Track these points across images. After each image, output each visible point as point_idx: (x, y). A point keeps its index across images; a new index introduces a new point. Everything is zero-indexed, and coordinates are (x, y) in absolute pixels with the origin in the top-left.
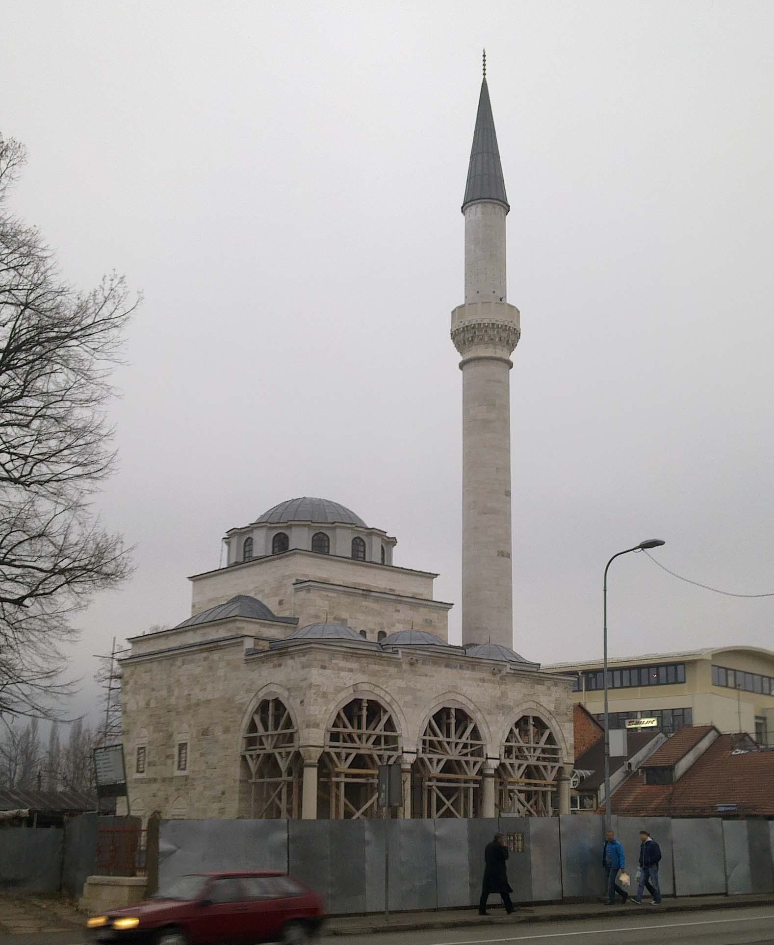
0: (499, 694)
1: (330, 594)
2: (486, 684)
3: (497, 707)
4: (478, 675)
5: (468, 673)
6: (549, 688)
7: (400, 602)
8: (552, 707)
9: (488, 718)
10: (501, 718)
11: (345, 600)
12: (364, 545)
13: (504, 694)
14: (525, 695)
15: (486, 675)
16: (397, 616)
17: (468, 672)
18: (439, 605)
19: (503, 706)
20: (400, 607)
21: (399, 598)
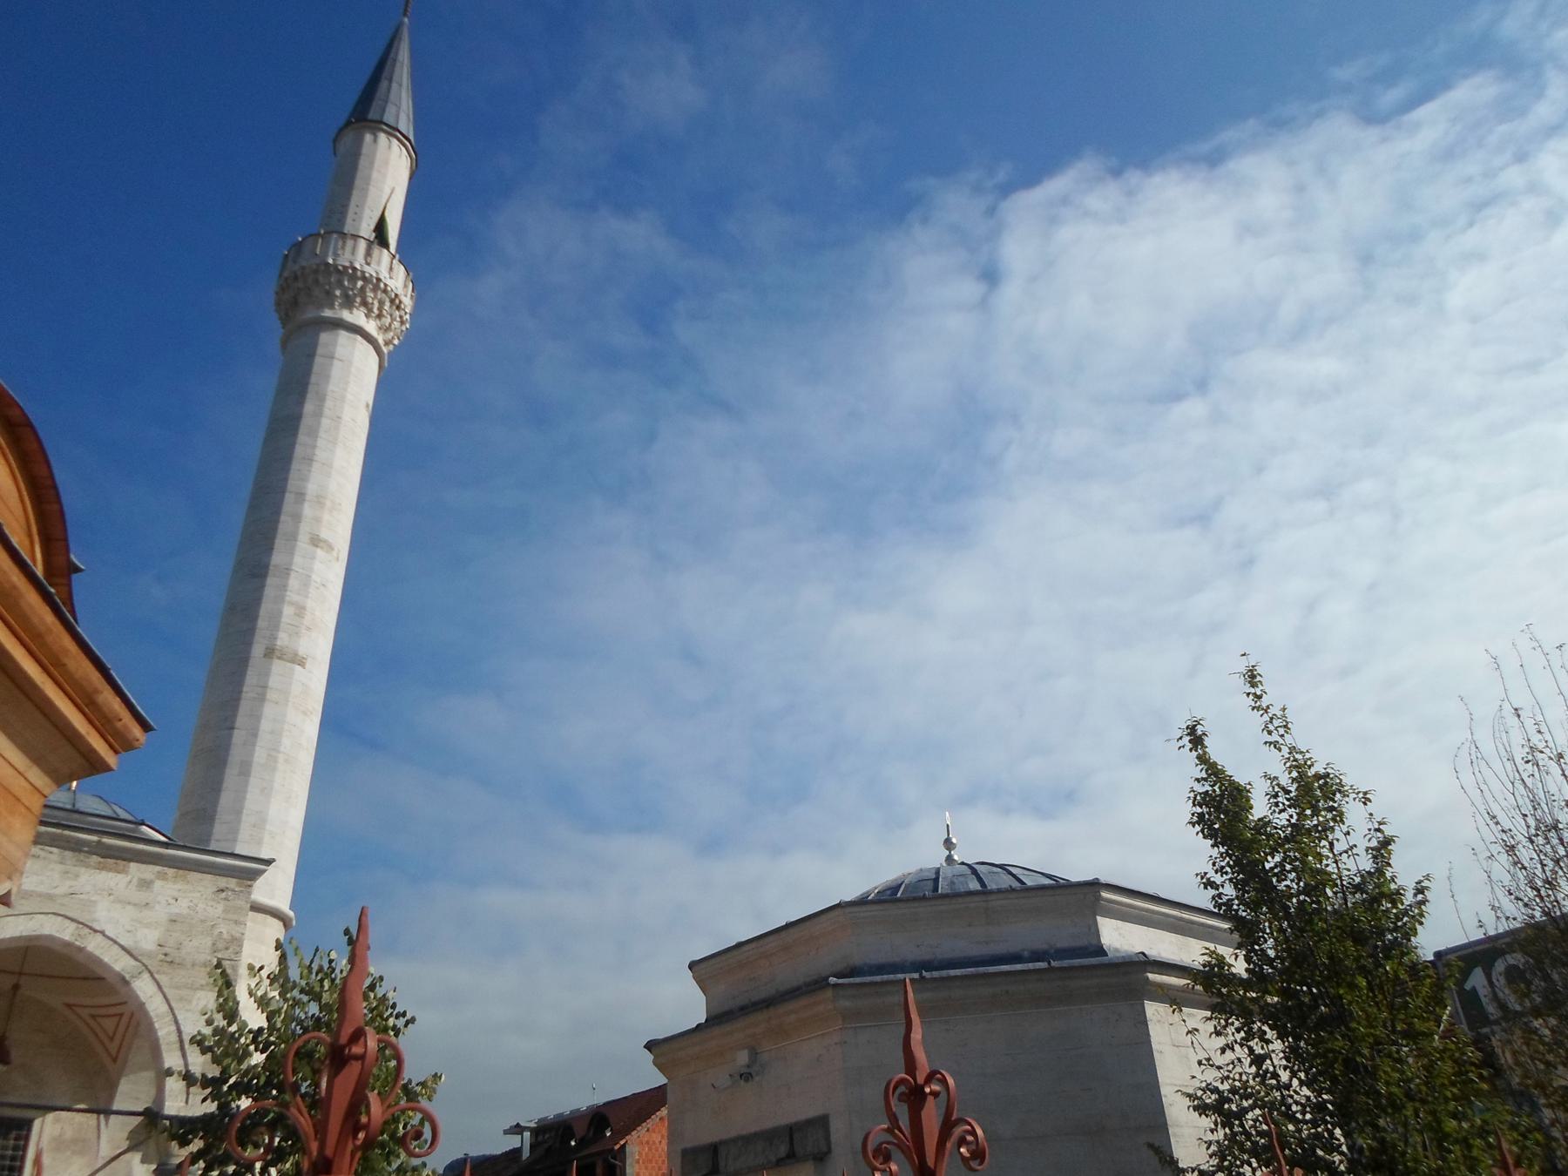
6: (145, 884)
8: (147, 940)
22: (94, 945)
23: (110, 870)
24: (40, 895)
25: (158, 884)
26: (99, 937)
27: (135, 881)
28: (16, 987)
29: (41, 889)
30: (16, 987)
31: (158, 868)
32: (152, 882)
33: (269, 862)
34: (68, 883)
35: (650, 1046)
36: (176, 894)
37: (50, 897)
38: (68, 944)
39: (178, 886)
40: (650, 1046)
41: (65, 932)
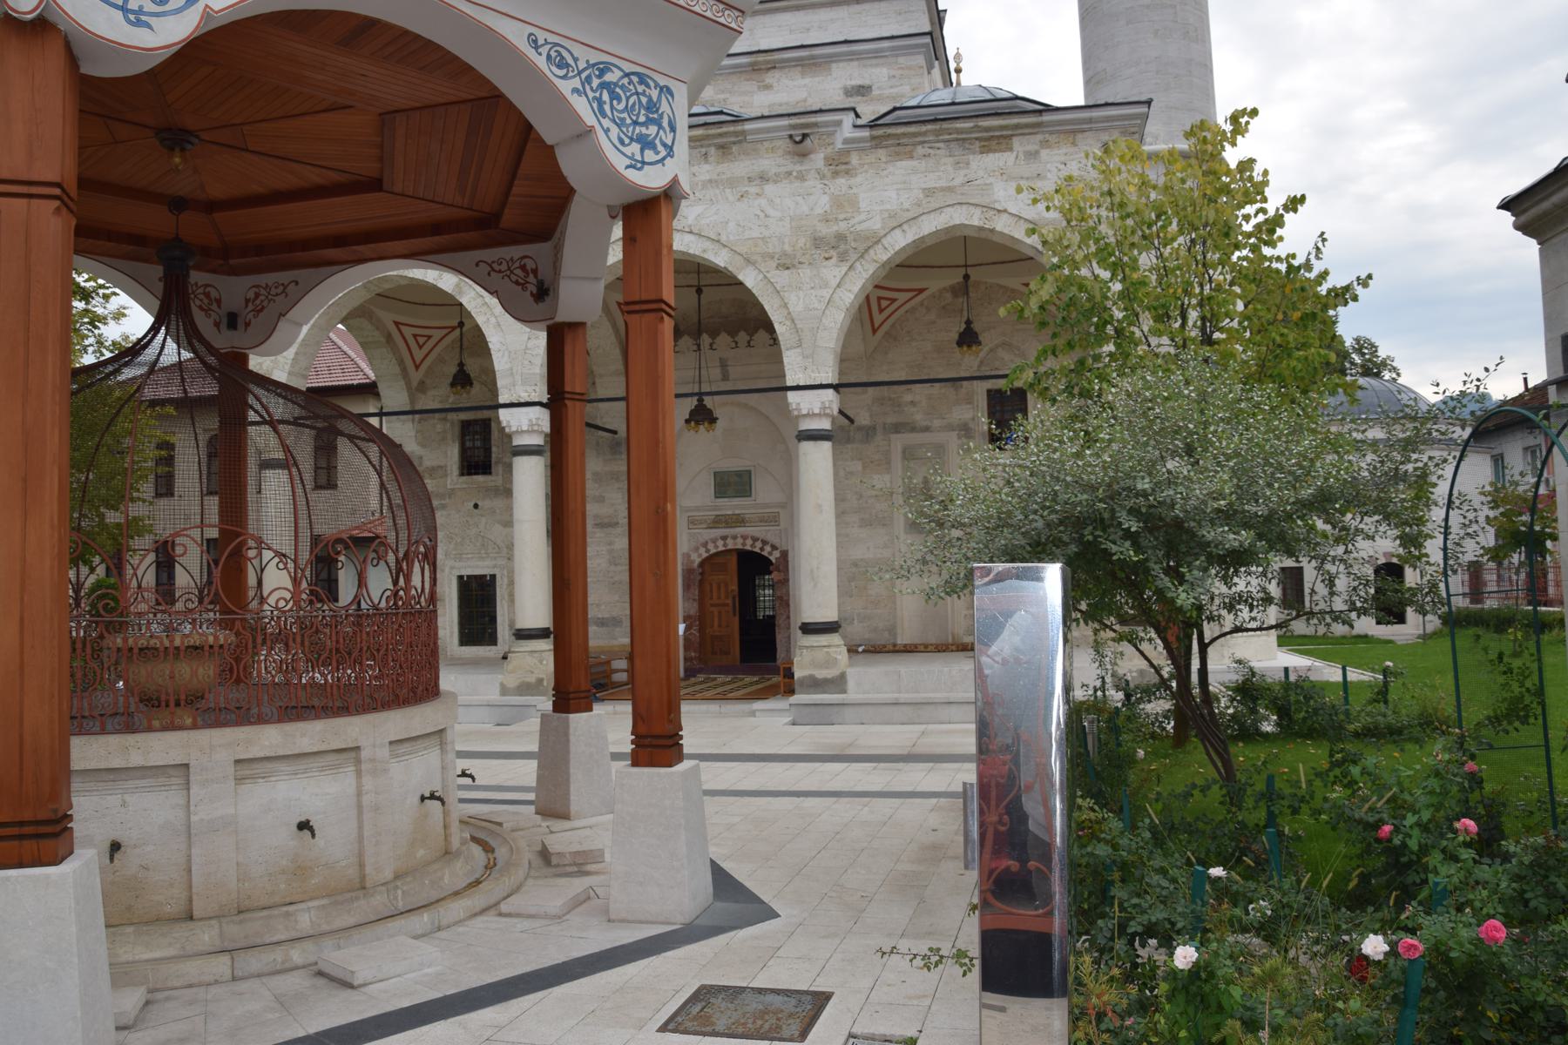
0: (823, 203)
2: (769, 189)
3: (818, 242)
4: (740, 167)
6: (1032, 156)
9: (781, 278)
10: (833, 272)
13: (844, 204)
14: (929, 192)
15: (771, 161)
17: (707, 167)
18: (886, 44)
19: (841, 237)
20: (771, 78)
21: (761, 58)
22: (1002, 225)
23: (995, 151)
24: (943, 189)
25: (1044, 153)
26: (1005, 216)
27: (1021, 156)
28: (966, 277)
29: (943, 183)
30: (966, 277)
31: (1039, 137)
32: (1037, 152)
33: (1149, 103)
34: (962, 172)
35: (1506, 205)
36: (1063, 159)
37: (950, 189)
38: (981, 229)
39: (1064, 150)
40: (1506, 205)
41: (975, 218)
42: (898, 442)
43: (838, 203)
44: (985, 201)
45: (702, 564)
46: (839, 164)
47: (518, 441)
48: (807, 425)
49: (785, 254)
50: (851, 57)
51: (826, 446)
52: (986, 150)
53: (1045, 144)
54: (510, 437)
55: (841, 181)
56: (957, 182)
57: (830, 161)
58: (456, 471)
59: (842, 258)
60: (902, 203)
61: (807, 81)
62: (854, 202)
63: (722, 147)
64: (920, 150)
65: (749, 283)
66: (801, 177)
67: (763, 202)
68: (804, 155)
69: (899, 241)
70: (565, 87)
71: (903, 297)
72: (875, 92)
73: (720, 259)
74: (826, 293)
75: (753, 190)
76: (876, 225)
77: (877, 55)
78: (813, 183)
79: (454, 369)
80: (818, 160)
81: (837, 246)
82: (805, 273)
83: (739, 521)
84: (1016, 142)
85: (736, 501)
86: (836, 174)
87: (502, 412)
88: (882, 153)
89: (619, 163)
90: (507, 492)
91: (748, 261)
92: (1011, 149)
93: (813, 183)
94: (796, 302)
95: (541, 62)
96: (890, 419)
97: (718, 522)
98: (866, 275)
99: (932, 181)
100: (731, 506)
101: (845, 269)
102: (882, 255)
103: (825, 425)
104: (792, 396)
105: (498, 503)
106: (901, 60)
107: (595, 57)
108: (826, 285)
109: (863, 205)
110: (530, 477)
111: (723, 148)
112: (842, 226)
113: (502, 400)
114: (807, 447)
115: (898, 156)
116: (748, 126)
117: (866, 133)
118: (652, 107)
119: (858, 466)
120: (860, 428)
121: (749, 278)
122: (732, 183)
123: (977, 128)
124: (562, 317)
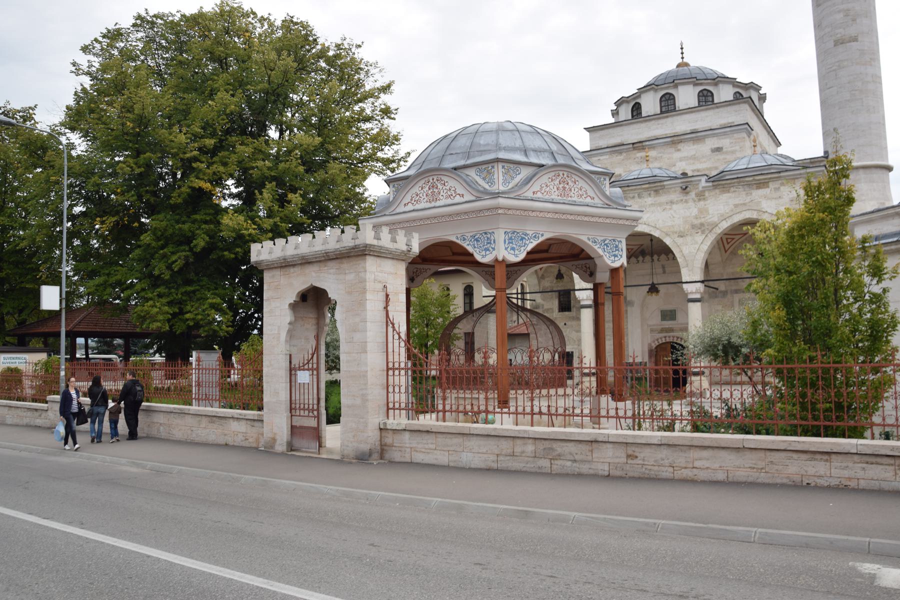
0: (695, 211)
1: (601, 158)
2: (674, 206)
3: (693, 226)
4: (663, 198)
5: (649, 200)
6: (777, 189)
7: (681, 141)
9: (680, 241)
10: (699, 238)
11: (618, 158)
12: (674, 99)
14: (736, 206)
15: (675, 196)
16: (677, 155)
19: (702, 225)
20: (680, 146)
21: (675, 138)
25: (782, 188)
29: (742, 202)
37: (744, 204)
42: (737, 297)
43: (701, 211)
44: (758, 208)
45: (656, 348)
46: (701, 196)
47: (582, 303)
48: (691, 296)
49: (680, 232)
50: (714, 135)
51: (699, 304)
52: (758, 188)
53: (782, 184)
54: (579, 301)
55: (702, 203)
56: (747, 201)
57: (697, 195)
58: (557, 310)
59: (703, 232)
60: (724, 210)
61: (695, 146)
62: (707, 211)
63: (656, 191)
64: (732, 189)
65: (668, 243)
66: (686, 202)
67: (672, 211)
68: (687, 193)
69: (725, 225)
70: (596, 247)
71: (737, 237)
72: (724, 150)
73: (656, 234)
74: (697, 246)
75: (668, 207)
76: (715, 219)
77: (725, 134)
78: (691, 204)
79: (556, 273)
80: (693, 194)
81: (700, 228)
82: (689, 239)
83: (671, 330)
84: (771, 184)
85: (670, 322)
86: (700, 200)
87: (576, 292)
88: (717, 191)
89: (609, 262)
90: (578, 319)
91: (667, 235)
92: (768, 187)
93: (691, 204)
94: (686, 250)
95: (590, 243)
96: (734, 288)
97: (663, 330)
98: (712, 239)
99: (737, 201)
100: (668, 324)
101: (704, 236)
102: (718, 231)
103: (698, 296)
104: (685, 286)
105: (574, 323)
106: (735, 135)
107: (602, 238)
108: (697, 243)
109: (710, 212)
110: (587, 317)
111: (656, 191)
112: (703, 220)
113: (576, 288)
114: (691, 305)
115: (723, 192)
116: (665, 183)
117: (711, 184)
118: (617, 246)
119: (720, 307)
120: (721, 292)
121: (668, 241)
122: (660, 204)
123: (754, 180)
124: (597, 281)
